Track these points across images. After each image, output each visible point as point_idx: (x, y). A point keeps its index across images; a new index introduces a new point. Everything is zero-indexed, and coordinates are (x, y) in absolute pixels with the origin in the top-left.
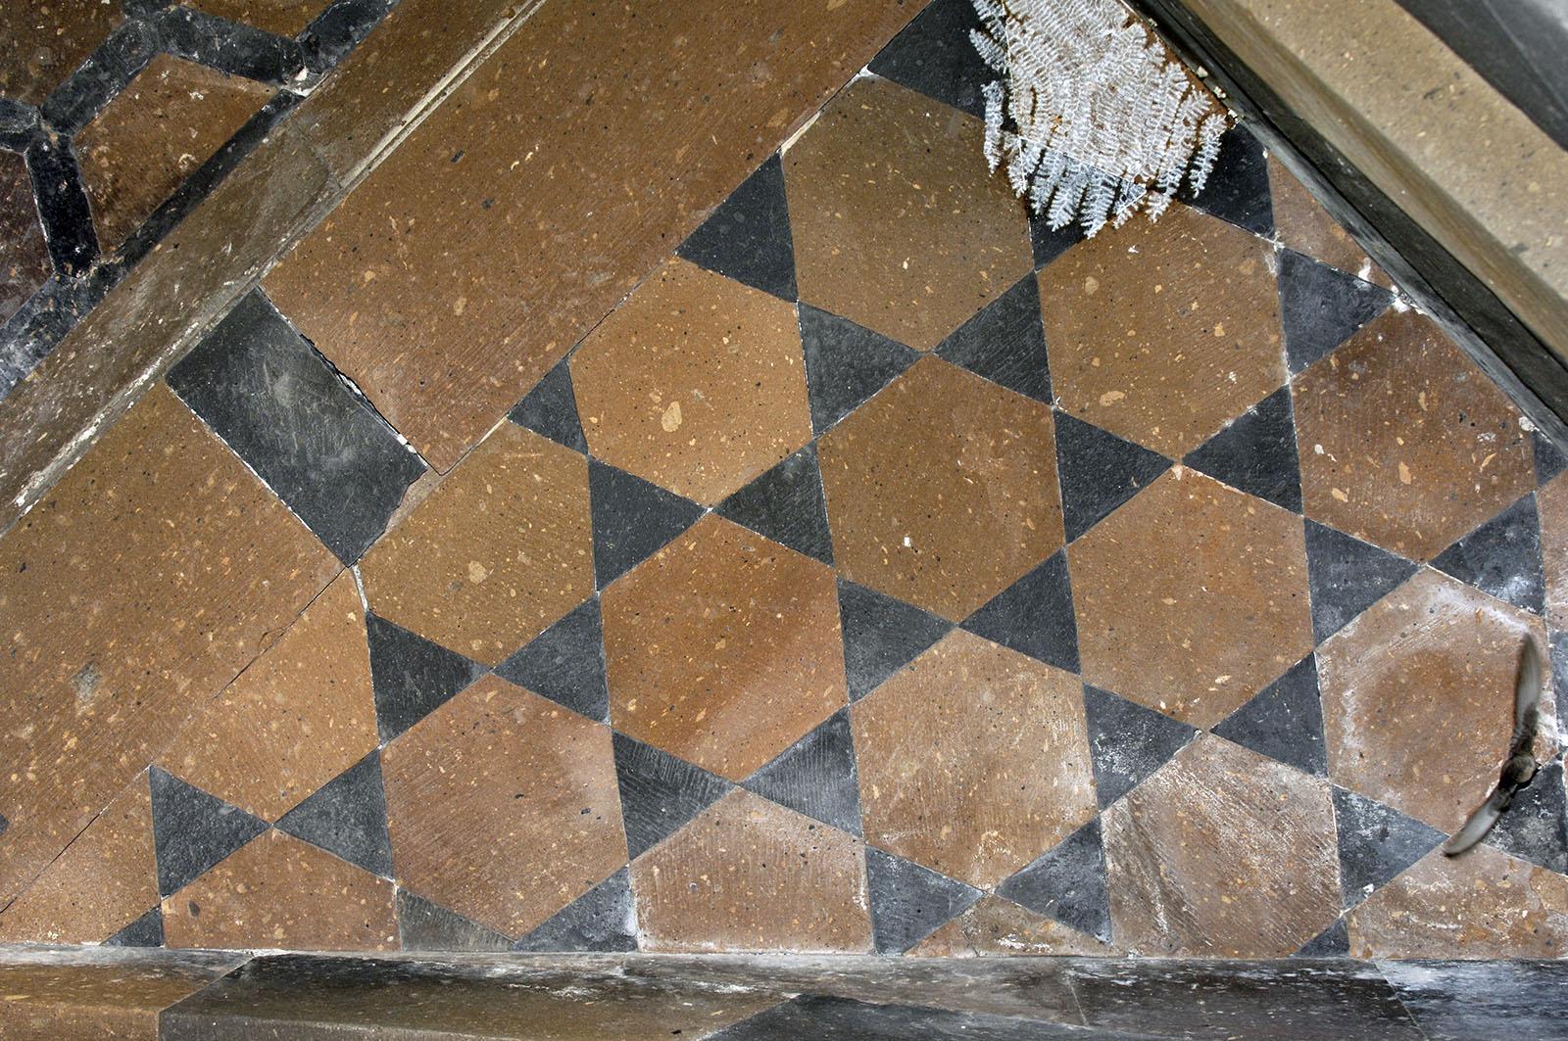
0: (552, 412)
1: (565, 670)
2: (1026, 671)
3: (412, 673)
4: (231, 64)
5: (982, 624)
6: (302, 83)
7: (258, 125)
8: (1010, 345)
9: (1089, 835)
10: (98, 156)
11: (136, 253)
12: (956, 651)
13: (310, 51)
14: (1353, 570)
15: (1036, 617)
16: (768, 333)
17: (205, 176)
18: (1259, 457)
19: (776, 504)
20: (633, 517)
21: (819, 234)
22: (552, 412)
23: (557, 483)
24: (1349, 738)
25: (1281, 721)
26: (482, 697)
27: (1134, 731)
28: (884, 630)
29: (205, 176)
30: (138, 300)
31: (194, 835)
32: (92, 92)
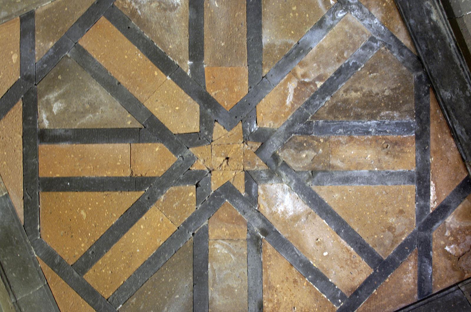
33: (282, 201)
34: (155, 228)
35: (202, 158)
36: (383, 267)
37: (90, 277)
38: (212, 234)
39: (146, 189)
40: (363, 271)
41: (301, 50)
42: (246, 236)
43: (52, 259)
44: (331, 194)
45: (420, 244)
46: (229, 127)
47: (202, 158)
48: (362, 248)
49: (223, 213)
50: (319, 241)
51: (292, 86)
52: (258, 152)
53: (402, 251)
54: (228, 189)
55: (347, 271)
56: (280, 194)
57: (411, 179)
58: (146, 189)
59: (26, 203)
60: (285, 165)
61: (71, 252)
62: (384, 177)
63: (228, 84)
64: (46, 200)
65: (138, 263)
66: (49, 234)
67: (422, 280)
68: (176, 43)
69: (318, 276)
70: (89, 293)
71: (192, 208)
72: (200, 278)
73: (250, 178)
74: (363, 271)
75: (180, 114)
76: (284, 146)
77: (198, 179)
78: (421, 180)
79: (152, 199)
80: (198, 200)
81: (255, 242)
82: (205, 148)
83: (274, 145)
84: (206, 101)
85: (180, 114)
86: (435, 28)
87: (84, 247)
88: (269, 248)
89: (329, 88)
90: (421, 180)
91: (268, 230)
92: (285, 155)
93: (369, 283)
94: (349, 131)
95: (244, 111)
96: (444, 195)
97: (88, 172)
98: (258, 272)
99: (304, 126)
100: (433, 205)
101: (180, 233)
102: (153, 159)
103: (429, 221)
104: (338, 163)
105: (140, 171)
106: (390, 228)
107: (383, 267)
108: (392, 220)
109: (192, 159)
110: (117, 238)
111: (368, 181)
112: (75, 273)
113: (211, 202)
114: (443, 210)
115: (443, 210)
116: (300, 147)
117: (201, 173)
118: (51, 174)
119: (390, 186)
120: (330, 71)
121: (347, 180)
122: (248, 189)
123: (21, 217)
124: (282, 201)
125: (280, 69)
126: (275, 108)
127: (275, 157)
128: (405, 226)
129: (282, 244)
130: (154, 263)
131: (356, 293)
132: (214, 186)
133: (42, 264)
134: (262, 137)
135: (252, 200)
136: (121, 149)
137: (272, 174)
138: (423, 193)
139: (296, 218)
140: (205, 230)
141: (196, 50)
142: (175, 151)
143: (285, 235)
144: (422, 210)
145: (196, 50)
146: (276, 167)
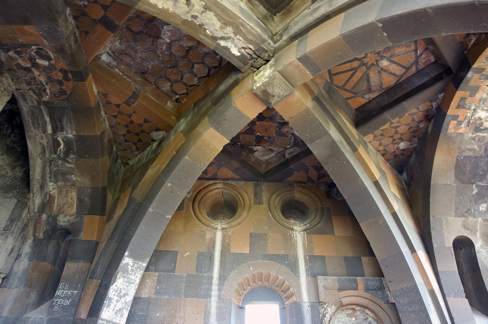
0: (134, 112)
1: (120, 113)
2: (126, 132)
3: (118, 106)
4: (155, 82)
5: (128, 130)
6: (154, 86)
7: (151, 83)
8: (143, 131)
9: (118, 134)
10: (148, 75)
11: (142, 77)
12: (126, 129)
13: (156, 86)
14: (135, 144)
15: (129, 132)
16: (141, 122)
17: (148, 81)
18: (140, 140)
19: (132, 122)
20: (130, 116)
21: (147, 124)
22: (134, 112)
23: (131, 112)
24: (126, 143)
25: (126, 141)
26: (118, 109)
27: (124, 135)
28: (127, 126)
29: (148, 81)
30: (139, 79)
31: (105, 95)
32: (152, 75)
33: (385, 63)
34: (358, 75)
37: (346, 87)
38: (370, 74)
39: (355, 70)
40: (404, 70)
42: (377, 72)
43: (337, 86)
44: (395, 59)
45: (416, 62)
48: (403, 67)
49: (372, 69)
50: (394, 68)
52: (378, 56)
53: (412, 65)
54: (372, 64)
56: (384, 62)
57: (413, 51)
58: (355, 70)
59: (330, 79)
60: (384, 57)
61: (341, 84)
64: (334, 77)
65: (355, 83)
66: (336, 82)
67: (417, 68)
69: (394, 74)
70: (346, 90)
71: (365, 70)
72: (368, 81)
73: (377, 61)
74: (404, 70)
76: (384, 53)
77: (365, 65)
79: (356, 71)
80: (366, 68)
81: (380, 72)
82: (366, 58)
83: (381, 53)
87: (343, 83)
88: (382, 72)
91: (382, 69)
92: (384, 55)
93: (405, 72)
94: (398, 46)
96: (421, 52)
97: (342, 70)
98: (381, 77)
101: (363, 75)
102: (355, 64)
103: (417, 58)
104: (396, 53)
105: (352, 67)
106: (409, 61)
109: (364, 61)
110: (350, 79)
111: (403, 54)
112: (343, 88)
113: (369, 68)
114: (421, 54)
115: (421, 54)
116: (387, 52)
117: (366, 63)
118: (334, 73)
119: (409, 53)
121: (399, 55)
122: (377, 63)
123: (330, 82)
124: (385, 63)
127: (382, 56)
128: (412, 60)
129: (385, 71)
130: (358, 82)
133: (335, 88)
135: (378, 65)
136: (349, 64)
137: (382, 59)
138: (416, 52)
139: (388, 65)
140: (368, 73)
144: (416, 56)
146: (382, 58)
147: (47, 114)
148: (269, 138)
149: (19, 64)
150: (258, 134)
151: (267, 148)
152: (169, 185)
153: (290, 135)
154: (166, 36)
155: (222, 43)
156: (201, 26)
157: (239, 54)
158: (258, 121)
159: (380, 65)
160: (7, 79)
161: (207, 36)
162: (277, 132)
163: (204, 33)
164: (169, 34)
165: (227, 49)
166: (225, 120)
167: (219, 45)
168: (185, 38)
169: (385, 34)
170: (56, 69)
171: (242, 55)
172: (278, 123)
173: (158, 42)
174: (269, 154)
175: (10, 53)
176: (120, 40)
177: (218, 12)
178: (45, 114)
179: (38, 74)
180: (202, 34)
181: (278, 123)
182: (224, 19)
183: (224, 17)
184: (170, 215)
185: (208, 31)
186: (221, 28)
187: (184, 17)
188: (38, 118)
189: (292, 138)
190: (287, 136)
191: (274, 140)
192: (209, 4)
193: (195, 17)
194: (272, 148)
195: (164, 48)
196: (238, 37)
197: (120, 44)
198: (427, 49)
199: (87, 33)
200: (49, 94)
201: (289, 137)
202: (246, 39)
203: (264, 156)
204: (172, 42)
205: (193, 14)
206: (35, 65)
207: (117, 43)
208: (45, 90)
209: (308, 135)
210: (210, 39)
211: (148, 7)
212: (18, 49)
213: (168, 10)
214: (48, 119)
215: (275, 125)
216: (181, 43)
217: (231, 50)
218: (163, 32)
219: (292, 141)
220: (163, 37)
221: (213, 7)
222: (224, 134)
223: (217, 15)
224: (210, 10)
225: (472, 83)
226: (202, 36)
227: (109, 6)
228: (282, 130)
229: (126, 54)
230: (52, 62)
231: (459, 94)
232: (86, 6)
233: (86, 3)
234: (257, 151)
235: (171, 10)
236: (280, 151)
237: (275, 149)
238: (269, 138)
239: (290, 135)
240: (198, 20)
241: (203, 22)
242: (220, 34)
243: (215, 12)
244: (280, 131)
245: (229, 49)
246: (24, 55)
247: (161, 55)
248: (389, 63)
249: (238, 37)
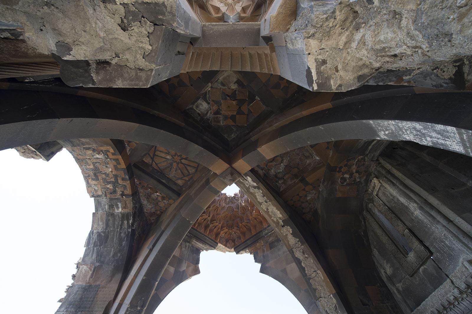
35: (179, 158)
36: (154, 155)
41: (176, 171)
46: (178, 162)
47: (179, 158)
48: (157, 156)
51: (175, 168)
53: (153, 157)
54: (175, 156)
55: (157, 153)
62: (160, 163)
63: (181, 165)
68: (189, 168)
69: (160, 151)
74: (156, 153)
75: (183, 161)
78: (156, 164)
80: (177, 154)
82: (180, 159)
84: (182, 163)
85: (183, 161)
86: (163, 180)
88: (168, 153)
89: (171, 168)
90: (156, 164)
91: (168, 154)
95: (178, 163)
96: (153, 164)
99: (171, 164)
100: (153, 162)
103: (153, 161)
107: (154, 155)
108: (157, 159)
109: (180, 157)
120: (172, 170)
125: (177, 169)
126: (175, 165)
129: (166, 153)
131: (155, 151)
132: (176, 156)
134: (175, 162)
137: (171, 159)
141: (185, 167)
142: (182, 158)
143: (166, 154)
144: (154, 161)
145: (186, 167)
147: (368, 149)
148: (226, 99)
149: (359, 175)
150: (234, 103)
151: (226, 87)
152: (308, 142)
153: (211, 102)
154: (282, 167)
155: (255, 184)
156: (264, 196)
157: (247, 177)
158: (235, 115)
159: (170, 156)
160: (372, 170)
161: (262, 190)
162: (221, 105)
163: (263, 192)
164: (280, 168)
165: (254, 181)
166: (258, 161)
167: (257, 184)
168: (273, 166)
169: (187, 219)
170: (343, 172)
171: (246, 177)
172: (221, 114)
173: (287, 163)
174: (224, 79)
175: (359, 180)
176: (305, 164)
177: (256, 201)
178: (369, 150)
179: (354, 170)
180: (264, 191)
181: (221, 114)
182: (254, 196)
183: (253, 197)
184: (319, 128)
185: (261, 192)
186: (255, 193)
187: (270, 203)
188: (376, 148)
189: (209, 99)
190: (213, 101)
191: (222, 97)
192: (259, 205)
193: (266, 202)
194: (222, 87)
195: (285, 161)
196: (248, 186)
197: (307, 162)
198: (151, 165)
199: (318, 180)
200: (357, 159)
201: (210, 100)
202: (244, 185)
203: (228, 76)
204: (280, 164)
205: (266, 204)
206: (351, 175)
207: (308, 162)
208: (358, 161)
209: (205, 154)
210: (261, 188)
211: (283, 214)
212: (353, 182)
213: (276, 209)
214: (370, 147)
215: (223, 112)
216: (276, 164)
217: (251, 180)
218: (283, 168)
219: (208, 96)
220: (284, 166)
221: (258, 203)
222: (260, 154)
223: (257, 199)
224: (259, 202)
225: (122, 172)
226: (265, 191)
227: (302, 190)
228: (217, 107)
229: (306, 157)
230: (342, 176)
231: (123, 166)
232: (312, 190)
233: (311, 191)
234: (235, 83)
235: (275, 208)
236: (215, 84)
237: (220, 86)
238: (226, 99)
239: (211, 102)
240: (265, 200)
241: (262, 198)
242: (256, 190)
243: (257, 201)
244: (218, 106)
245: (252, 180)
246: (353, 179)
247: (288, 157)
248: (166, 157)
249: (248, 186)
